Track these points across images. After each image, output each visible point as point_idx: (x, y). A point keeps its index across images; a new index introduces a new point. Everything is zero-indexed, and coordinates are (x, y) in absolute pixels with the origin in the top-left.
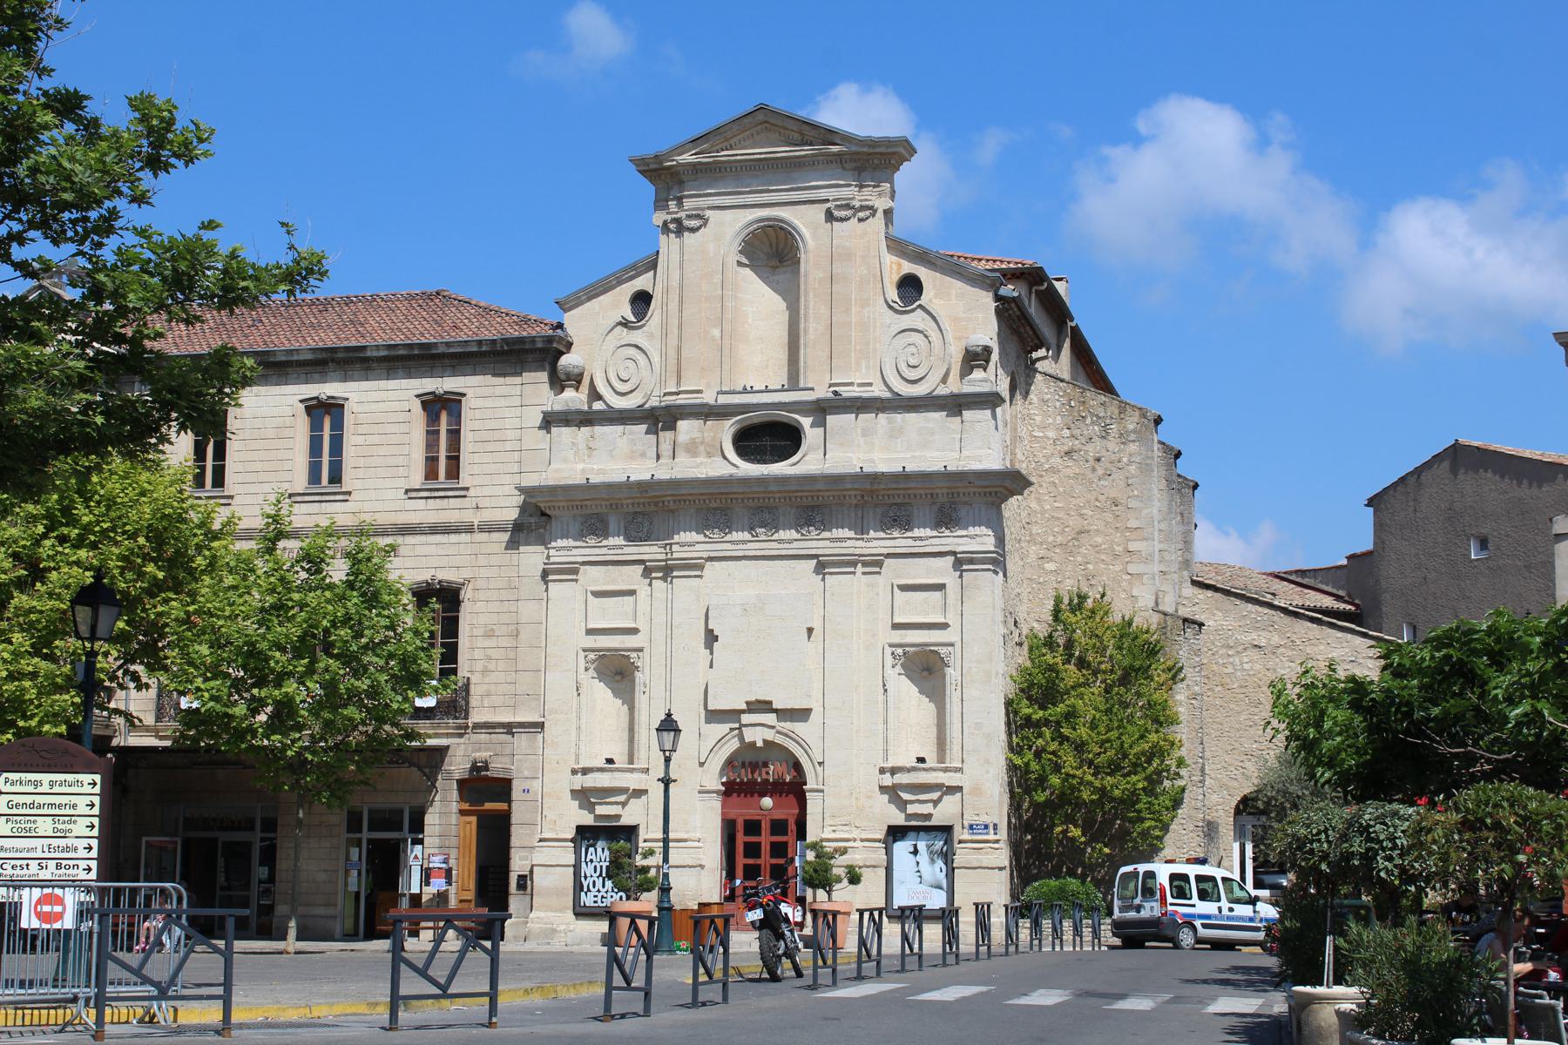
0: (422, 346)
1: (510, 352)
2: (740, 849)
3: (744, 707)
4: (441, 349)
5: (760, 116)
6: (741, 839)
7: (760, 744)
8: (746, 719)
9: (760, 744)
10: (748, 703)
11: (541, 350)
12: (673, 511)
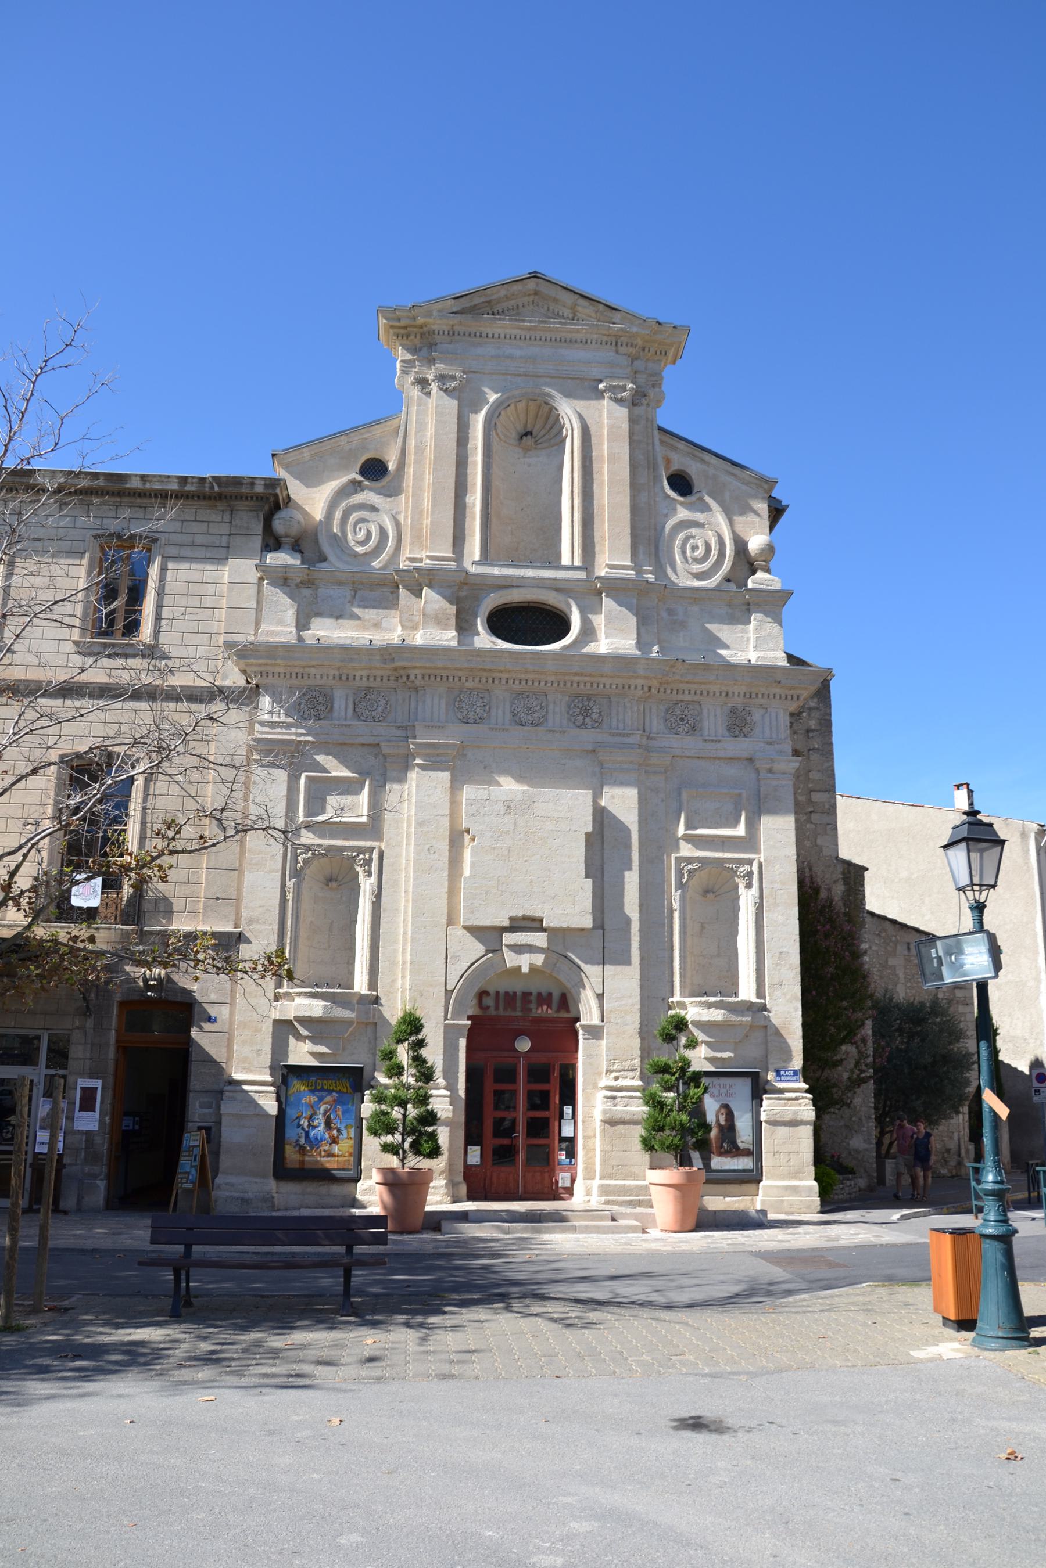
0: (109, 477)
1: (220, 497)
2: (489, 1099)
3: (506, 923)
4: (135, 484)
5: (532, 284)
6: (490, 1086)
7: (525, 970)
8: (508, 938)
9: (525, 970)
10: (511, 919)
11: (258, 498)
12: (416, 689)
